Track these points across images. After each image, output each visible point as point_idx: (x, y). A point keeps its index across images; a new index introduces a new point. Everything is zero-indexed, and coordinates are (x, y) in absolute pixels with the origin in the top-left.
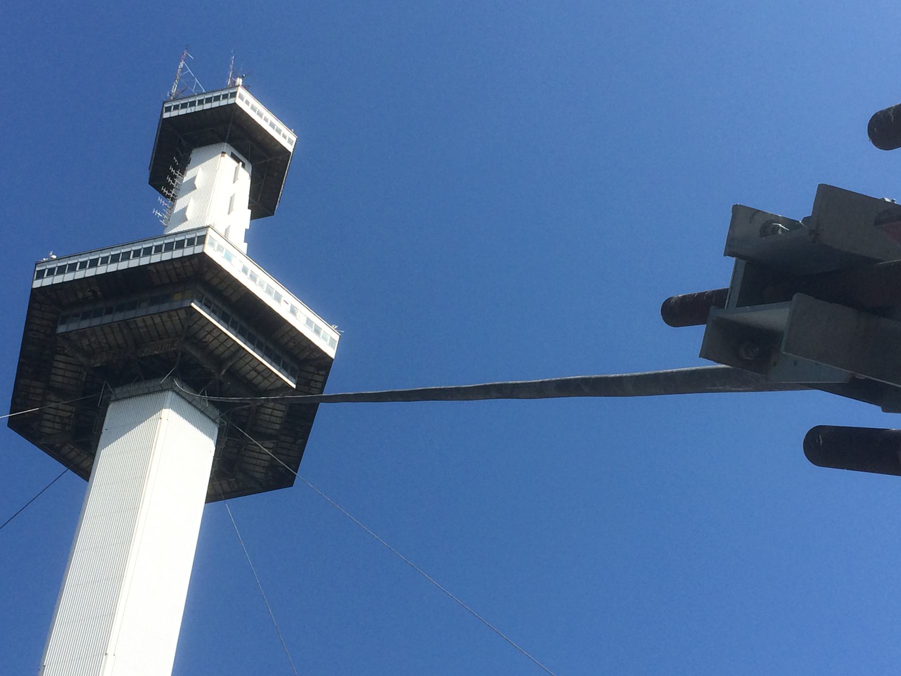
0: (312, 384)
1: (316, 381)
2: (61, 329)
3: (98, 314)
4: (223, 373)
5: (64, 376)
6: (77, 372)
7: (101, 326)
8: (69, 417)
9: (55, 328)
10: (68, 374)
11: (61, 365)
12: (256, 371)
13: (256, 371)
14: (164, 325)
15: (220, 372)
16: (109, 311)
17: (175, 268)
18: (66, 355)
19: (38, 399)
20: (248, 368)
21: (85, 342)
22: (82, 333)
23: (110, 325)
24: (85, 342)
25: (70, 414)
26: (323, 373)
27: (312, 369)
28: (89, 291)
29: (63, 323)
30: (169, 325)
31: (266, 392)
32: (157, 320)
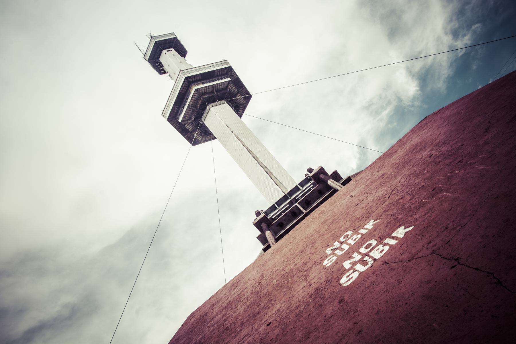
0: (233, 75)
1: (233, 73)
2: (180, 121)
3: (182, 110)
4: (215, 93)
5: (191, 128)
7: (186, 112)
9: (179, 122)
10: (191, 126)
11: (188, 126)
12: (221, 85)
13: (221, 85)
14: (195, 98)
15: (215, 94)
16: (184, 108)
17: (184, 86)
18: (186, 124)
20: (219, 87)
21: (187, 118)
22: (184, 117)
23: (187, 110)
24: (187, 118)
26: (232, 71)
27: (230, 73)
29: (179, 119)
30: (196, 97)
31: (227, 87)
32: (193, 99)
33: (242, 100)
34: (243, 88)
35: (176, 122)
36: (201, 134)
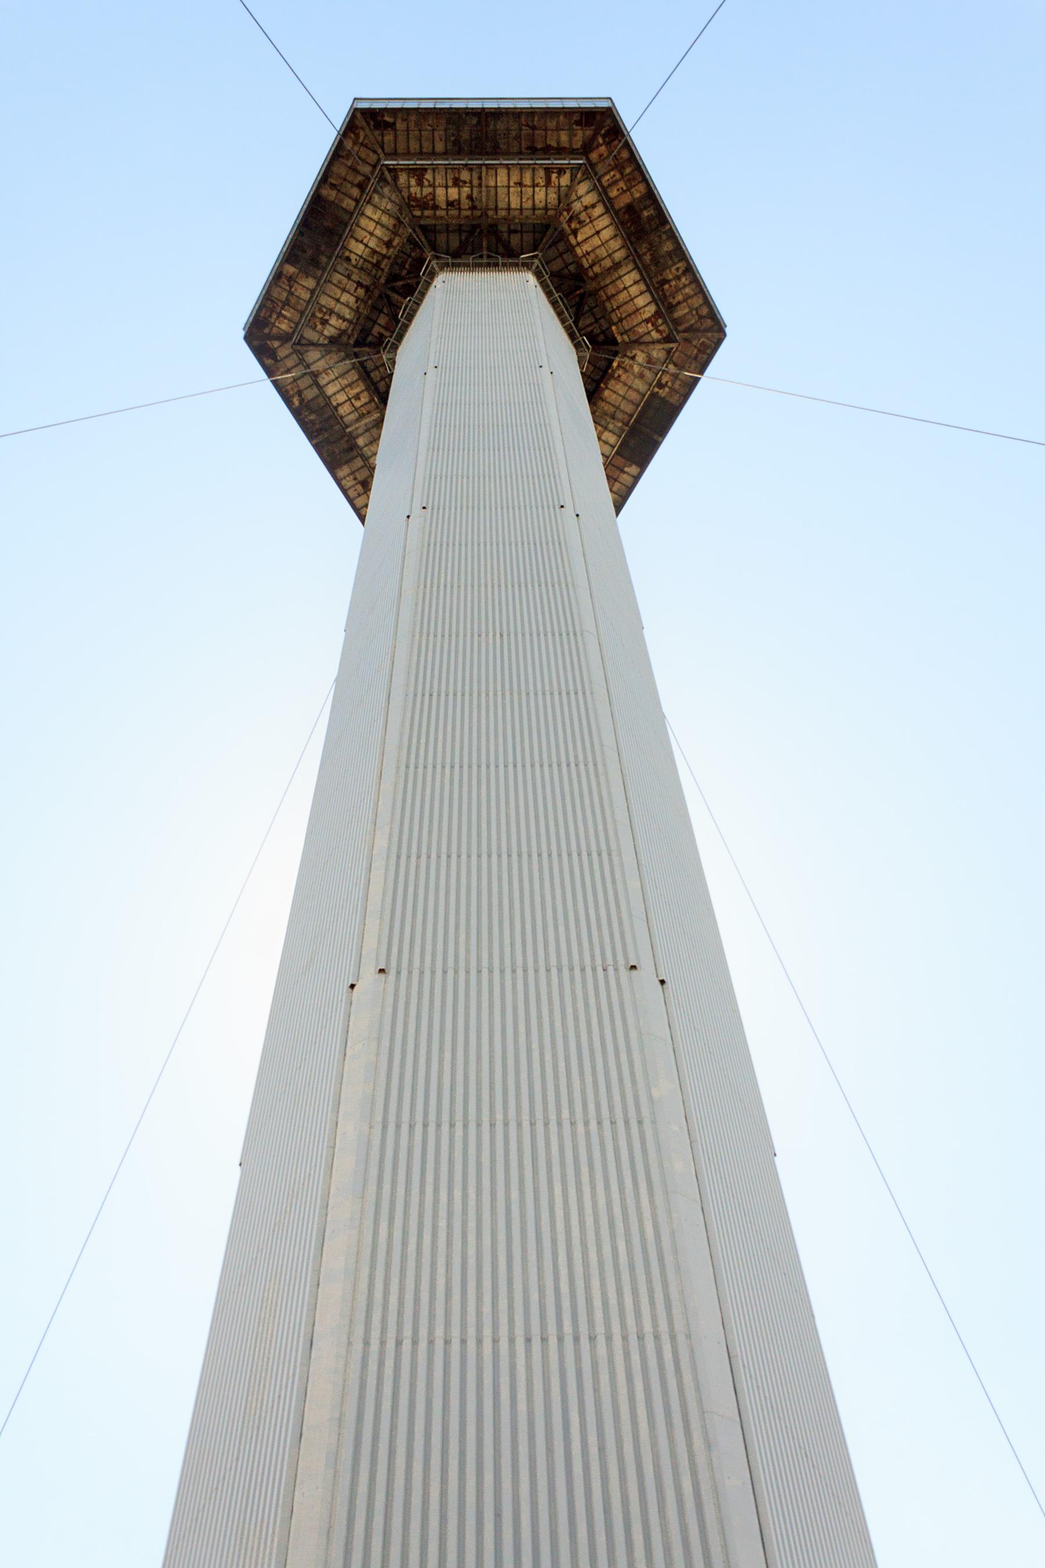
0: (359, 488)
1: (359, 495)
6: (618, 308)
8: (575, 233)
18: (647, 321)
19: (607, 177)
21: (641, 357)
24: (641, 357)
25: (580, 238)
28: (667, 382)
33: (325, 371)
34: (302, 401)
35: (679, 303)
36: (573, 226)
